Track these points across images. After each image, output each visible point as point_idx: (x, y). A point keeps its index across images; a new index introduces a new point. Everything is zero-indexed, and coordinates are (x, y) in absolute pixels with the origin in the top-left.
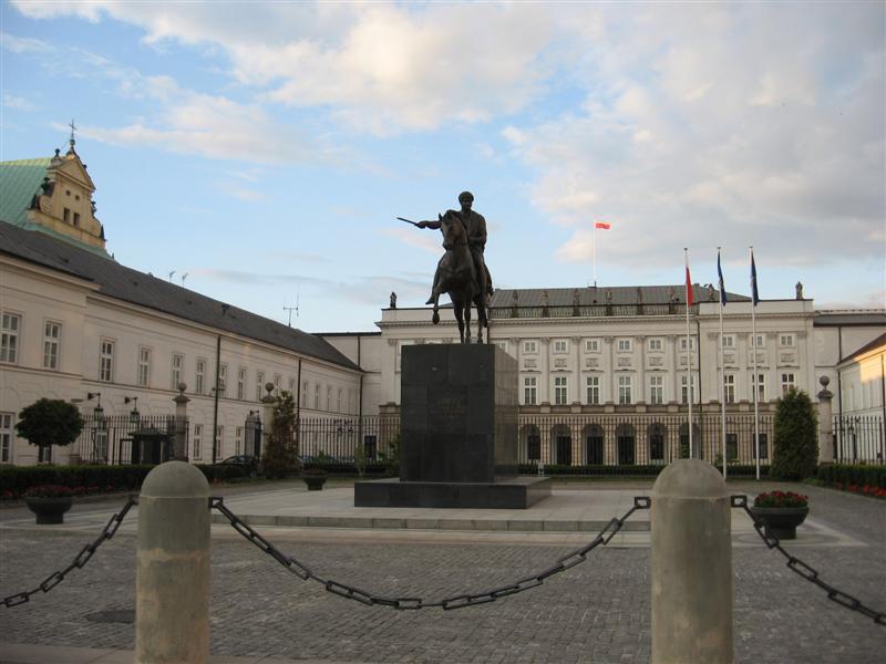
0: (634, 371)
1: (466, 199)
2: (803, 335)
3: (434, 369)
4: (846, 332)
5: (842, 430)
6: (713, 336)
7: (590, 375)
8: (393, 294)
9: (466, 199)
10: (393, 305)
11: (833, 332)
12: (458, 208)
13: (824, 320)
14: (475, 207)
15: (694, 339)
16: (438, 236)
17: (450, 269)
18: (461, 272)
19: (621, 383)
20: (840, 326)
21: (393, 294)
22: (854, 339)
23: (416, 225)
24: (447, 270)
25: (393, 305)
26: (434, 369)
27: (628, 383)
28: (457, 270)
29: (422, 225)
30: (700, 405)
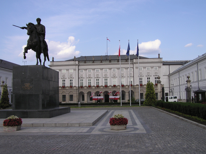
0: (100, 77)
1: (39, 20)
2: (160, 67)
4: (171, 66)
5: (170, 91)
6: (137, 68)
7: (97, 78)
8: (53, 57)
9: (39, 20)
10: (53, 60)
11: (168, 66)
12: (36, 23)
13: (165, 64)
14: (41, 23)
15: (132, 69)
16: (26, 31)
17: (31, 42)
18: (34, 42)
19: (97, 81)
20: (169, 65)
21: (53, 57)
22: (173, 68)
23: (21, 28)
24: (30, 42)
25: (53, 60)
27: (107, 80)
28: (33, 42)
29: (23, 28)
30: (134, 86)
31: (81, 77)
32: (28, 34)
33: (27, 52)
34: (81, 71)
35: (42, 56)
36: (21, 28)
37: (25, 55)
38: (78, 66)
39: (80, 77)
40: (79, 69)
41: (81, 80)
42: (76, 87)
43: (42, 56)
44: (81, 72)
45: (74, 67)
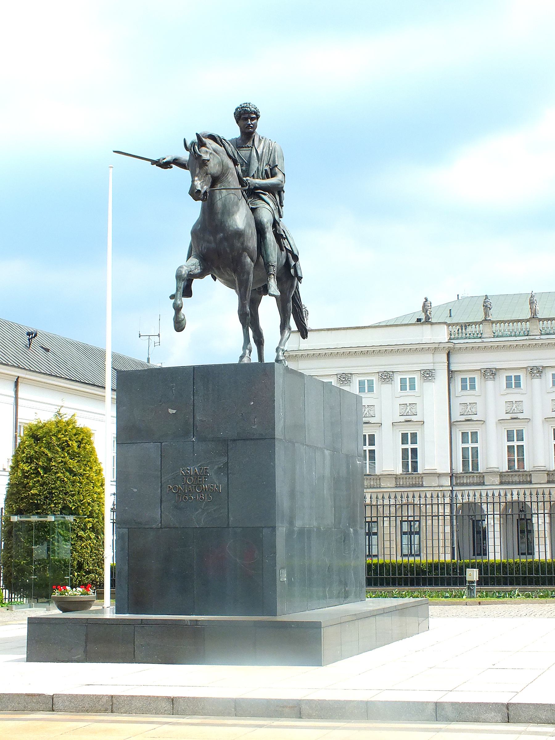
3: (171, 411)
9: (246, 117)
12: (232, 131)
14: (262, 129)
23: (154, 162)
26: (171, 411)
31: (463, 418)
32: (195, 194)
33: (187, 292)
34: (464, 380)
35: (268, 310)
36: (154, 162)
37: (178, 309)
38: (445, 356)
39: (456, 417)
40: (451, 374)
41: (464, 435)
42: (440, 475)
43: (268, 310)
44: (464, 388)
45: (425, 361)
